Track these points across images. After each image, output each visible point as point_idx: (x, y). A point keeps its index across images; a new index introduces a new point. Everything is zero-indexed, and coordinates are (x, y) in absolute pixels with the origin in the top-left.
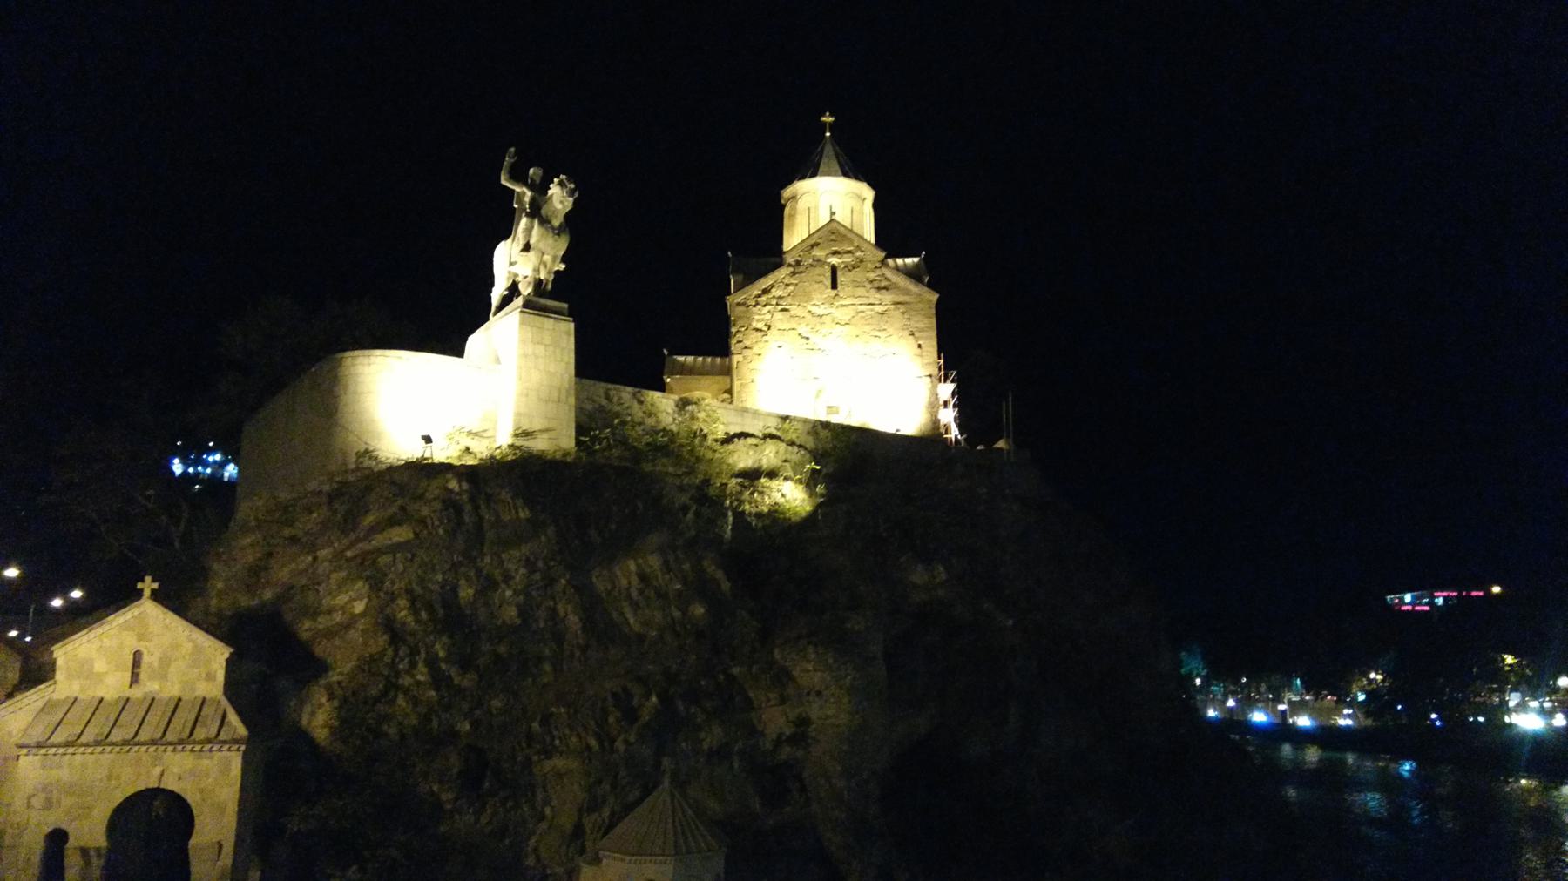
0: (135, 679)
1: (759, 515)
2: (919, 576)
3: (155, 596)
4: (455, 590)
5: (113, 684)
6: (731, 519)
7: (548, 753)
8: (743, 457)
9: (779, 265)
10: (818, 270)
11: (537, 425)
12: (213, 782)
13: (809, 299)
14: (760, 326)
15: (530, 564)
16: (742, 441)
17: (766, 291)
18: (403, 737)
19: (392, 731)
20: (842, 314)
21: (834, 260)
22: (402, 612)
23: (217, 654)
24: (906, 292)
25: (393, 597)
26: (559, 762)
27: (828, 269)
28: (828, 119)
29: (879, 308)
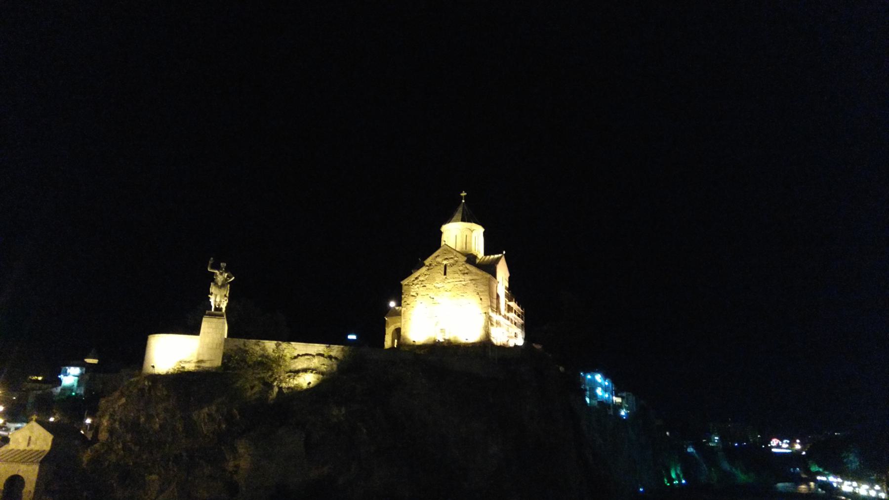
0: (29, 444)
1: (289, 388)
2: (335, 412)
3: (37, 421)
4: (139, 418)
5: (23, 446)
6: (276, 389)
7: (151, 474)
8: (300, 364)
9: (423, 265)
10: (438, 267)
11: (205, 358)
12: (30, 473)
13: (434, 279)
14: (414, 294)
15: (166, 410)
16: (302, 358)
17: (417, 278)
18: (109, 465)
19: (106, 463)
20: (448, 287)
21: (445, 262)
22: (117, 425)
23: (49, 437)
24: (476, 274)
25: (115, 421)
26: (154, 477)
27: (443, 267)
28: (464, 194)
29: (463, 283)
